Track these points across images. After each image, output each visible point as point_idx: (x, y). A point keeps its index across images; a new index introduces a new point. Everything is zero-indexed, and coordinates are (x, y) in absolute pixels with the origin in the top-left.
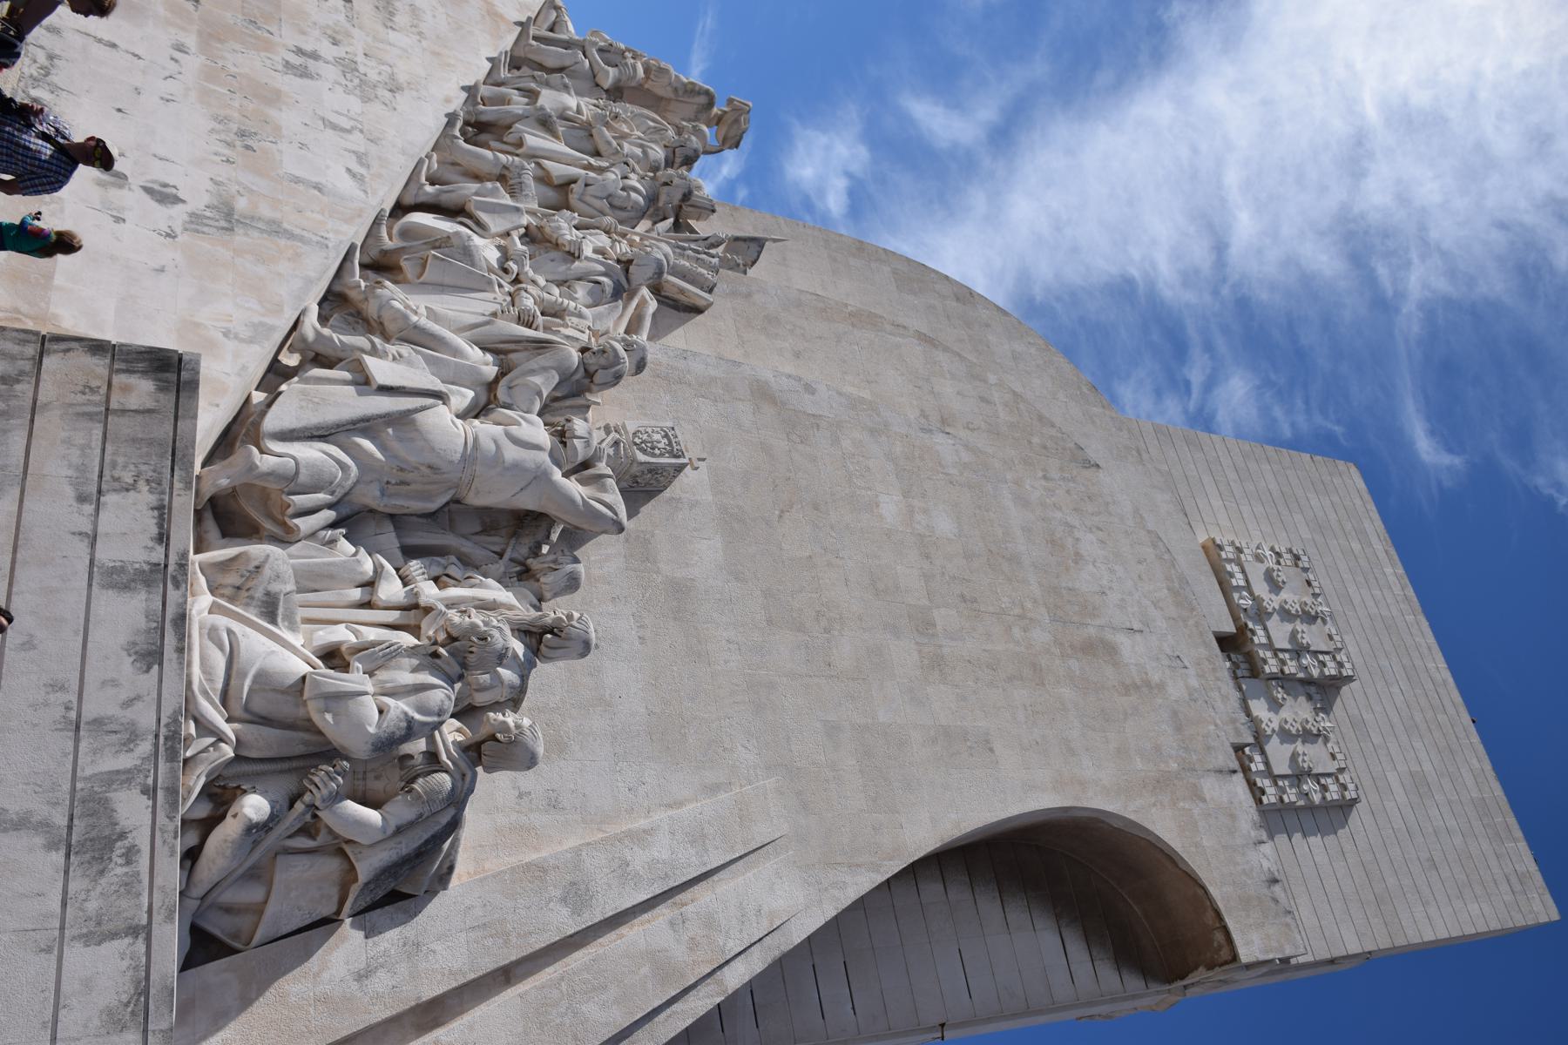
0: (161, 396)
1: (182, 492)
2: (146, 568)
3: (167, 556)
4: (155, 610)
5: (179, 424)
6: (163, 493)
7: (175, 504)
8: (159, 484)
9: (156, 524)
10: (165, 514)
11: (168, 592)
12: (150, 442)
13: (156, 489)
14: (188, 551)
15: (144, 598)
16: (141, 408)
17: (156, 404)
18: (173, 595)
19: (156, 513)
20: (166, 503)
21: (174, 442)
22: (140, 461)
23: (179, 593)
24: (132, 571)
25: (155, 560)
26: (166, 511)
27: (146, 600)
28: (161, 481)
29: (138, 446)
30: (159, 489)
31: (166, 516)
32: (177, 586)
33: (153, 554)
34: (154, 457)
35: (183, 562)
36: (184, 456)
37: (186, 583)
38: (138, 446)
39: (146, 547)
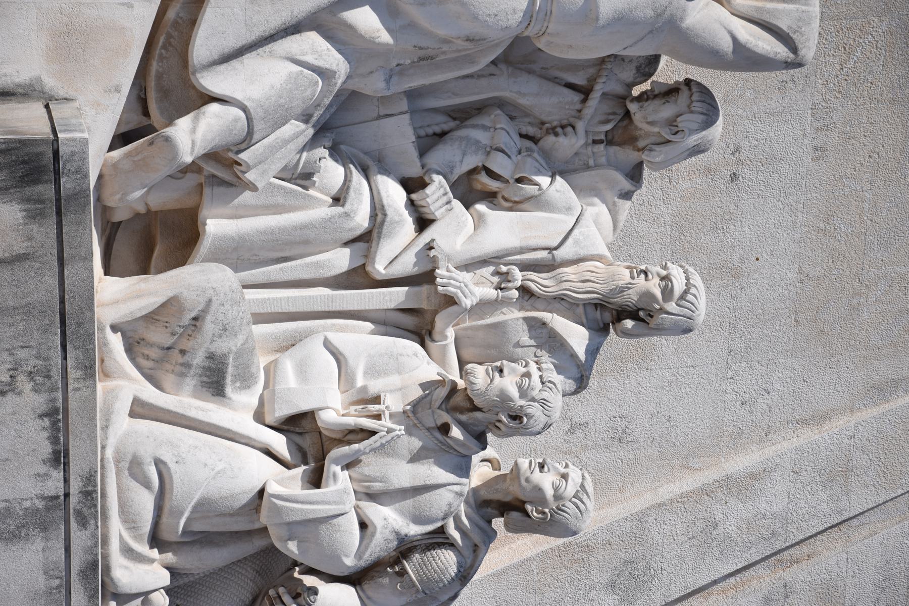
0: (34, 227)
1: (81, 384)
2: (40, 504)
3: (66, 481)
4: (56, 563)
5: (66, 273)
6: (53, 389)
7: (72, 404)
8: (46, 377)
9: (48, 438)
10: (59, 420)
11: (72, 534)
12: (27, 311)
13: (44, 384)
14: (96, 472)
15: (40, 548)
16: (7, 255)
17: (29, 244)
18: (79, 537)
19: (47, 422)
20: (59, 404)
21: (62, 301)
22: (16, 343)
23: (88, 532)
24: (20, 513)
25: (50, 492)
26: (61, 417)
27: (44, 550)
28: (49, 371)
29: (10, 320)
30: (48, 384)
31: (61, 424)
32: (83, 523)
33: (49, 483)
34: (35, 335)
35: (90, 488)
36: (79, 325)
37: (96, 518)
38: (10, 320)
39: (38, 475)
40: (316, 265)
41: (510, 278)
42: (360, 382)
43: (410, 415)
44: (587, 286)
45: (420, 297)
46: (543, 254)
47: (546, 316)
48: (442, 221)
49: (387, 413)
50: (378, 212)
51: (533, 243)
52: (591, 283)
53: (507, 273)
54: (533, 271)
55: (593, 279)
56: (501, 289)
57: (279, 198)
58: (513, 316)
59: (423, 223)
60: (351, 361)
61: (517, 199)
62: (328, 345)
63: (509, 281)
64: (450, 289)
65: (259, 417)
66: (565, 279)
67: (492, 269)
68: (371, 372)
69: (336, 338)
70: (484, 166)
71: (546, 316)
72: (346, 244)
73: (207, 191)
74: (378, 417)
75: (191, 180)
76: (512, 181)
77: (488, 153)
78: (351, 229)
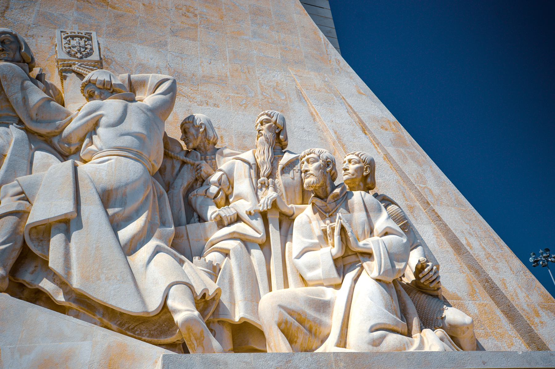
40: (259, 265)
41: (263, 183)
42: (316, 241)
43: (330, 214)
44: (266, 152)
45: (273, 217)
46: (252, 171)
47: (280, 167)
48: (237, 211)
49: (331, 224)
50: (233, 237)
51: (247, 174)
52: (265, 150)
53: (261, 184)
54: (260, 174)
55: (263, 150)
56: (268, 186)
57: (225, 281)
58: (280, 180)
59: (238, 219)
60: (307, 245)
61: (228, 184)
62: (299, 257)
63: (265, 183)
64: (269, 203)
65: (338, 286)
66: (263, 160)
67: (259, 190)
68: (310, 236)
69: (295, 253)
70: (213, 199)
71: (280, 167)
72: (249, 252)
73: (222, 318)
74: (333, 229)
75: (216, 327)
76: (220, 187)
77: (208, 197)
78: (241, 248)
